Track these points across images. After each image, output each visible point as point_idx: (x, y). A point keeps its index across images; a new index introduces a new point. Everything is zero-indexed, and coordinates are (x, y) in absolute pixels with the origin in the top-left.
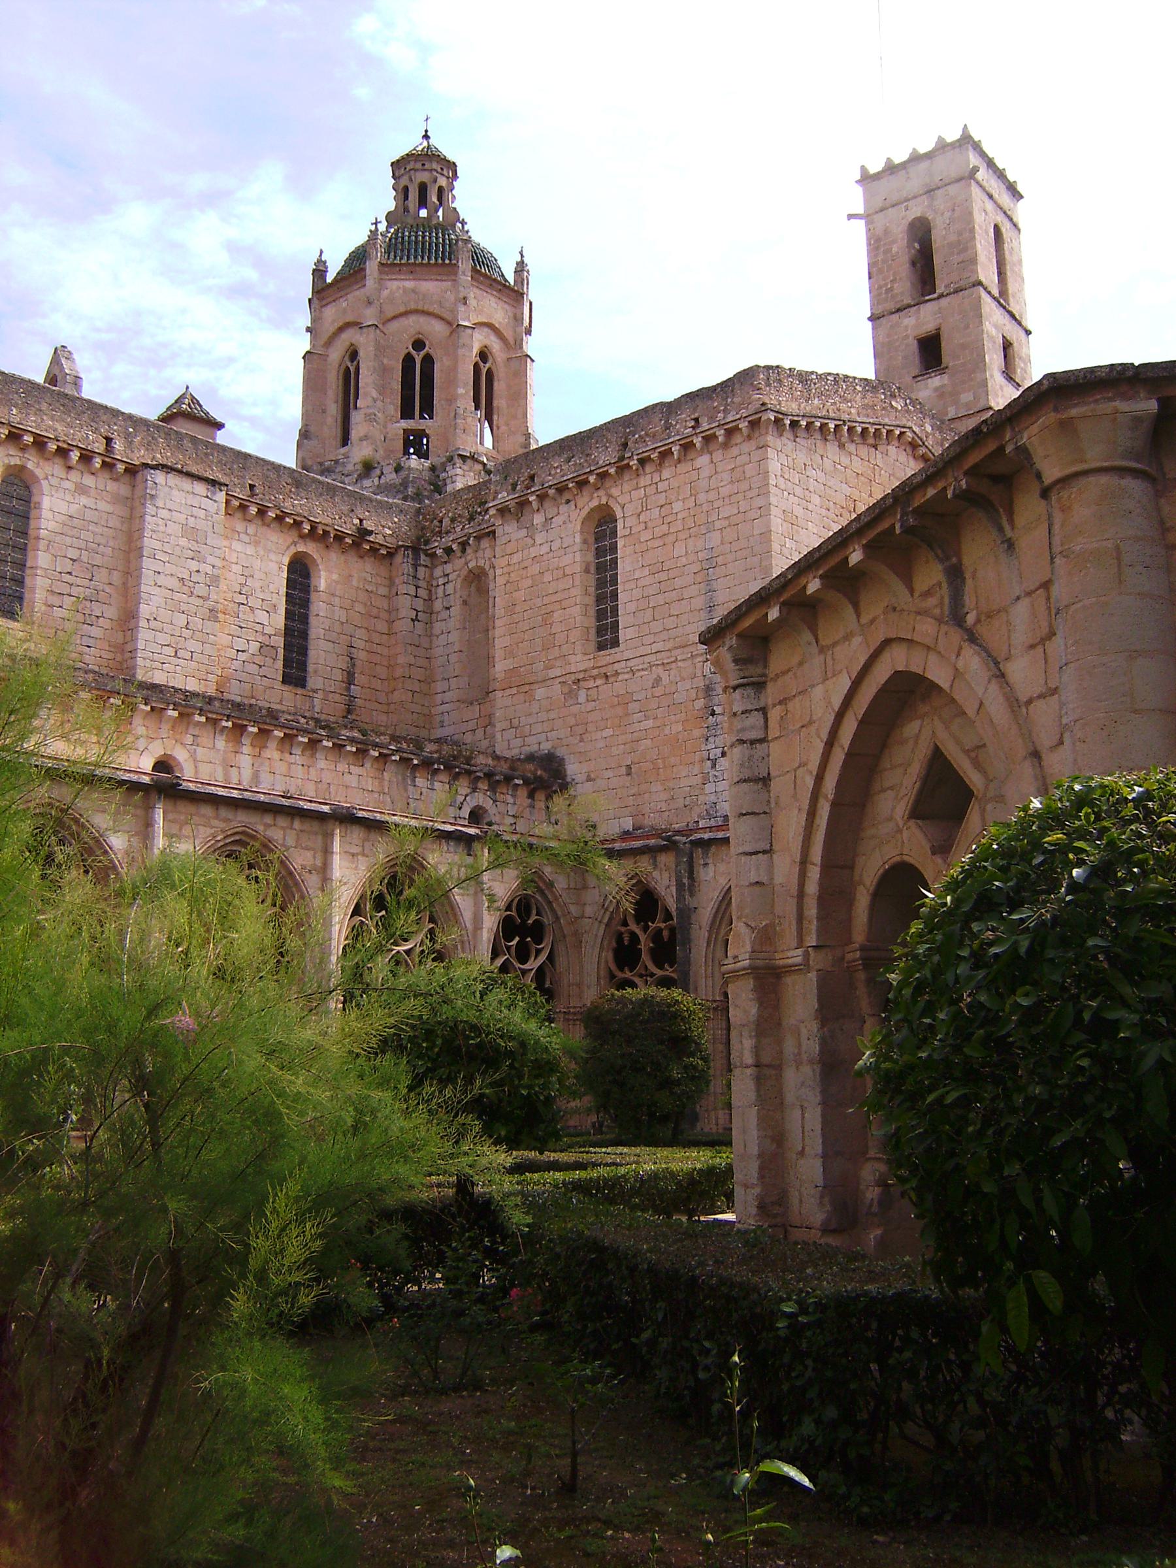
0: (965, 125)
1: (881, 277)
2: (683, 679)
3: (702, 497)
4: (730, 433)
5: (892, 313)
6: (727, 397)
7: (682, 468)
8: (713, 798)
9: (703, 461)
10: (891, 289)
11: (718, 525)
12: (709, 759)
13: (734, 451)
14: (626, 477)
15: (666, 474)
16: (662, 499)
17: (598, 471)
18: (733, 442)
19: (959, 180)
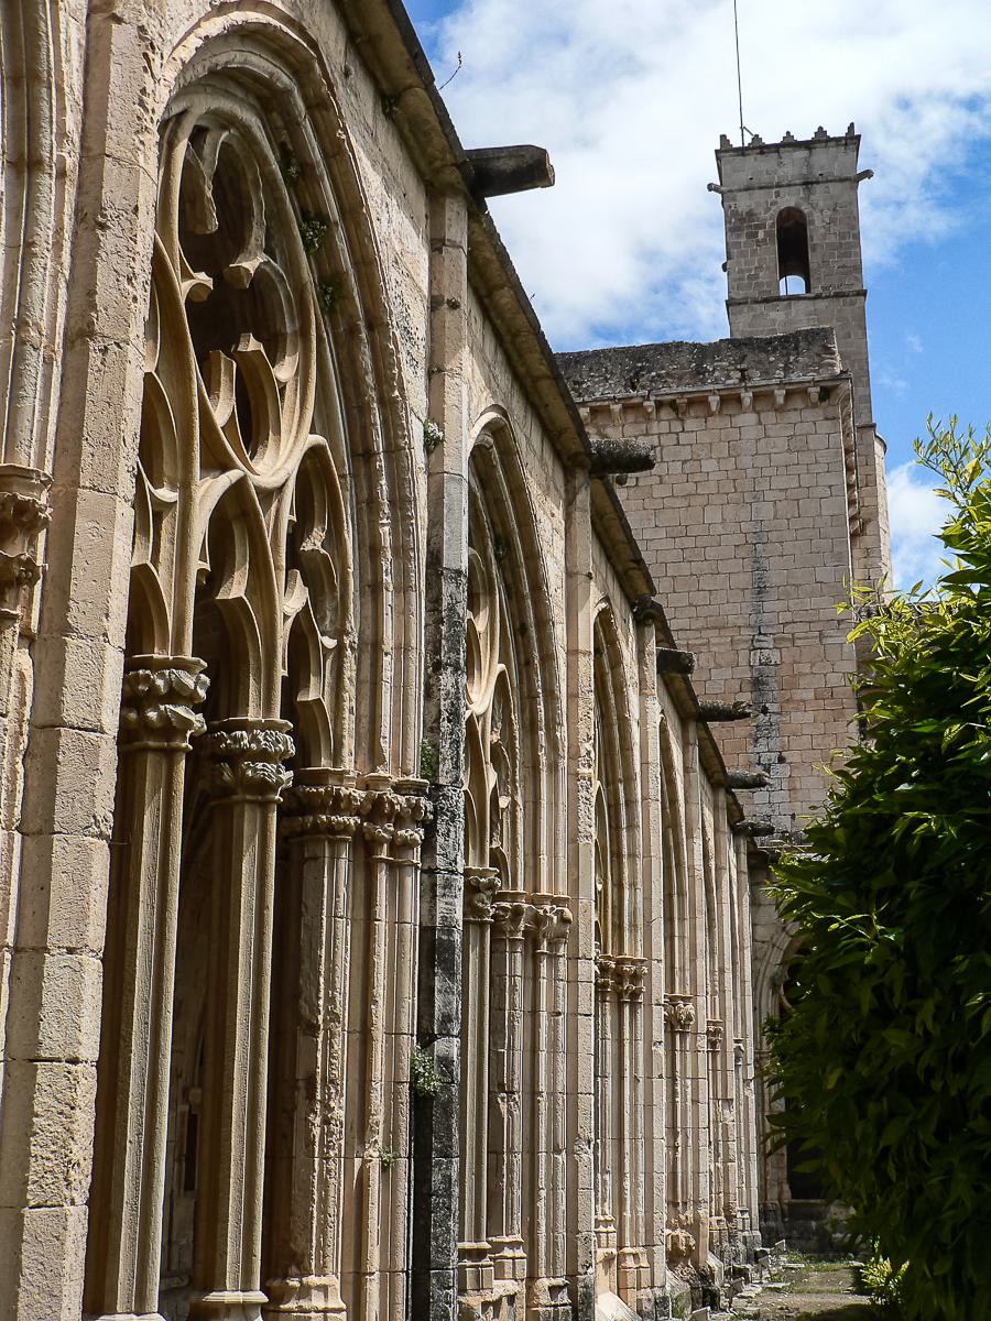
0: (852, 124)
1: (743, 260)
2: (718, 666)
3: (746, 461)
4: (789, 395)
5: (757, 302)
6: (788, 355)
7: (714, 422)
8: (766, 810)
9: (748, 419)
10: (756, 276)
11: (770, 496)
12: (759, 764)
13: (793, 417)
14: (631, 418)
15: (690, 424)
16: (686, 453)
17: (594, 404)
18: (791, 406)
19: (842, 180)
